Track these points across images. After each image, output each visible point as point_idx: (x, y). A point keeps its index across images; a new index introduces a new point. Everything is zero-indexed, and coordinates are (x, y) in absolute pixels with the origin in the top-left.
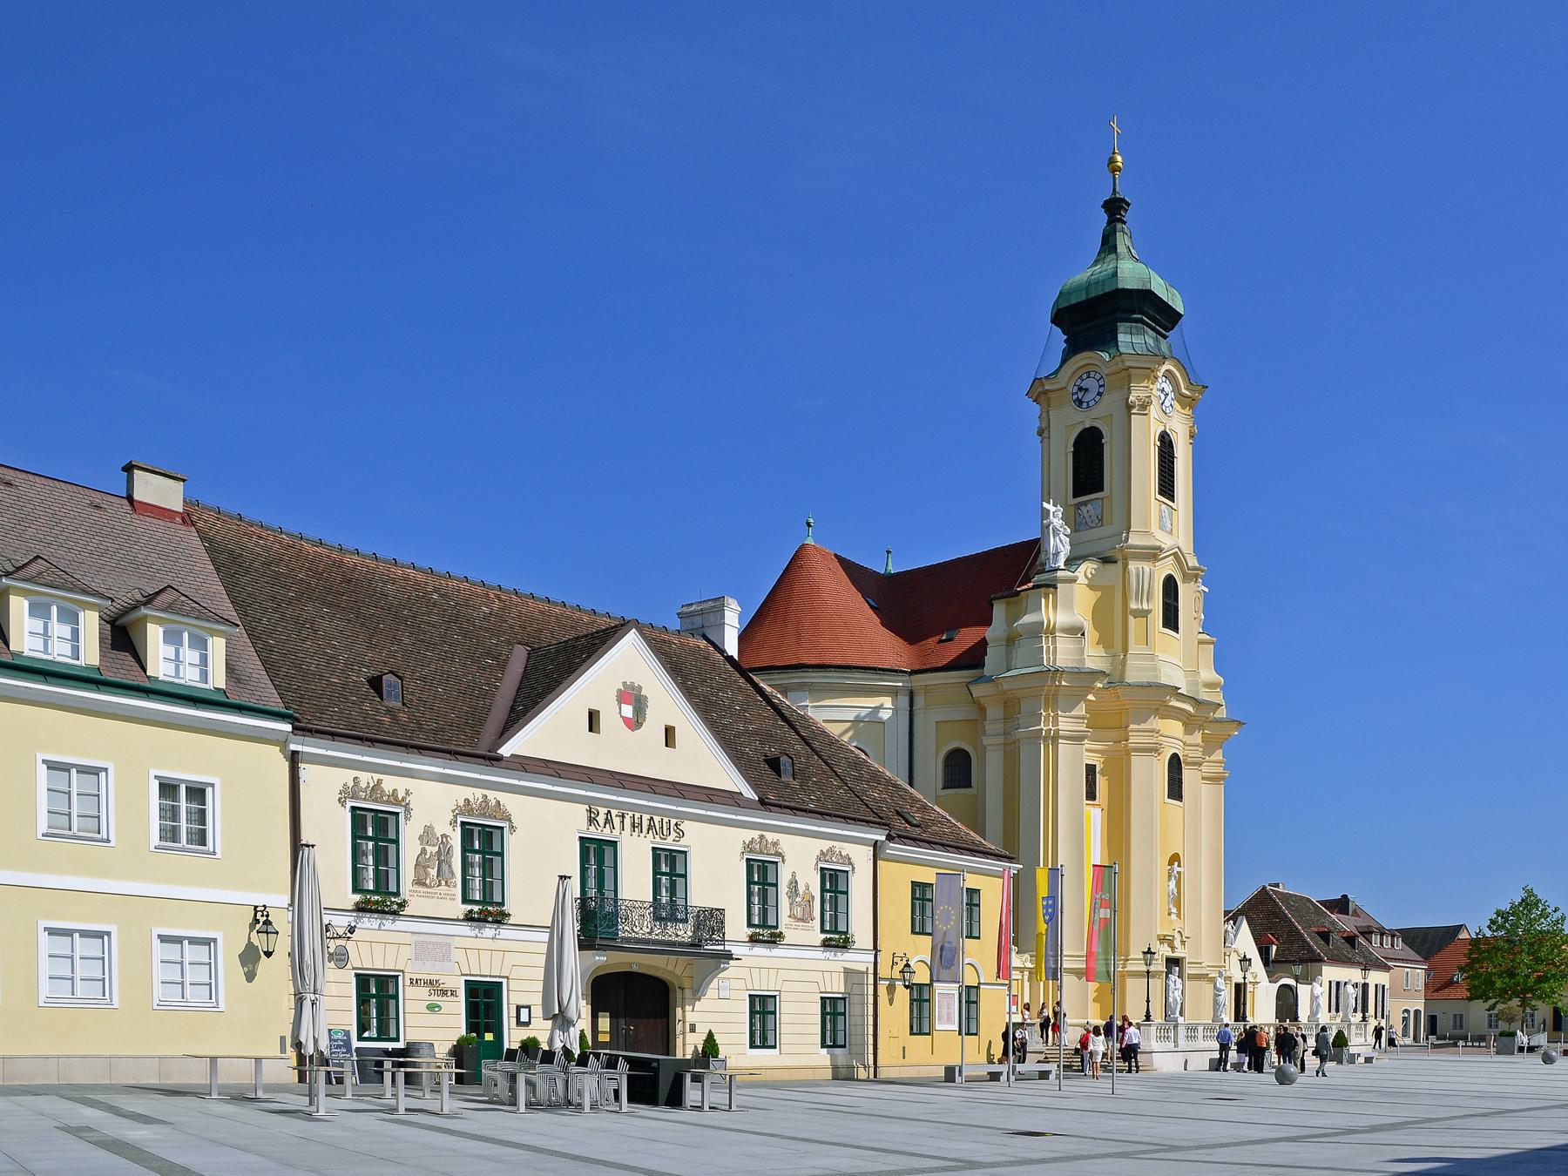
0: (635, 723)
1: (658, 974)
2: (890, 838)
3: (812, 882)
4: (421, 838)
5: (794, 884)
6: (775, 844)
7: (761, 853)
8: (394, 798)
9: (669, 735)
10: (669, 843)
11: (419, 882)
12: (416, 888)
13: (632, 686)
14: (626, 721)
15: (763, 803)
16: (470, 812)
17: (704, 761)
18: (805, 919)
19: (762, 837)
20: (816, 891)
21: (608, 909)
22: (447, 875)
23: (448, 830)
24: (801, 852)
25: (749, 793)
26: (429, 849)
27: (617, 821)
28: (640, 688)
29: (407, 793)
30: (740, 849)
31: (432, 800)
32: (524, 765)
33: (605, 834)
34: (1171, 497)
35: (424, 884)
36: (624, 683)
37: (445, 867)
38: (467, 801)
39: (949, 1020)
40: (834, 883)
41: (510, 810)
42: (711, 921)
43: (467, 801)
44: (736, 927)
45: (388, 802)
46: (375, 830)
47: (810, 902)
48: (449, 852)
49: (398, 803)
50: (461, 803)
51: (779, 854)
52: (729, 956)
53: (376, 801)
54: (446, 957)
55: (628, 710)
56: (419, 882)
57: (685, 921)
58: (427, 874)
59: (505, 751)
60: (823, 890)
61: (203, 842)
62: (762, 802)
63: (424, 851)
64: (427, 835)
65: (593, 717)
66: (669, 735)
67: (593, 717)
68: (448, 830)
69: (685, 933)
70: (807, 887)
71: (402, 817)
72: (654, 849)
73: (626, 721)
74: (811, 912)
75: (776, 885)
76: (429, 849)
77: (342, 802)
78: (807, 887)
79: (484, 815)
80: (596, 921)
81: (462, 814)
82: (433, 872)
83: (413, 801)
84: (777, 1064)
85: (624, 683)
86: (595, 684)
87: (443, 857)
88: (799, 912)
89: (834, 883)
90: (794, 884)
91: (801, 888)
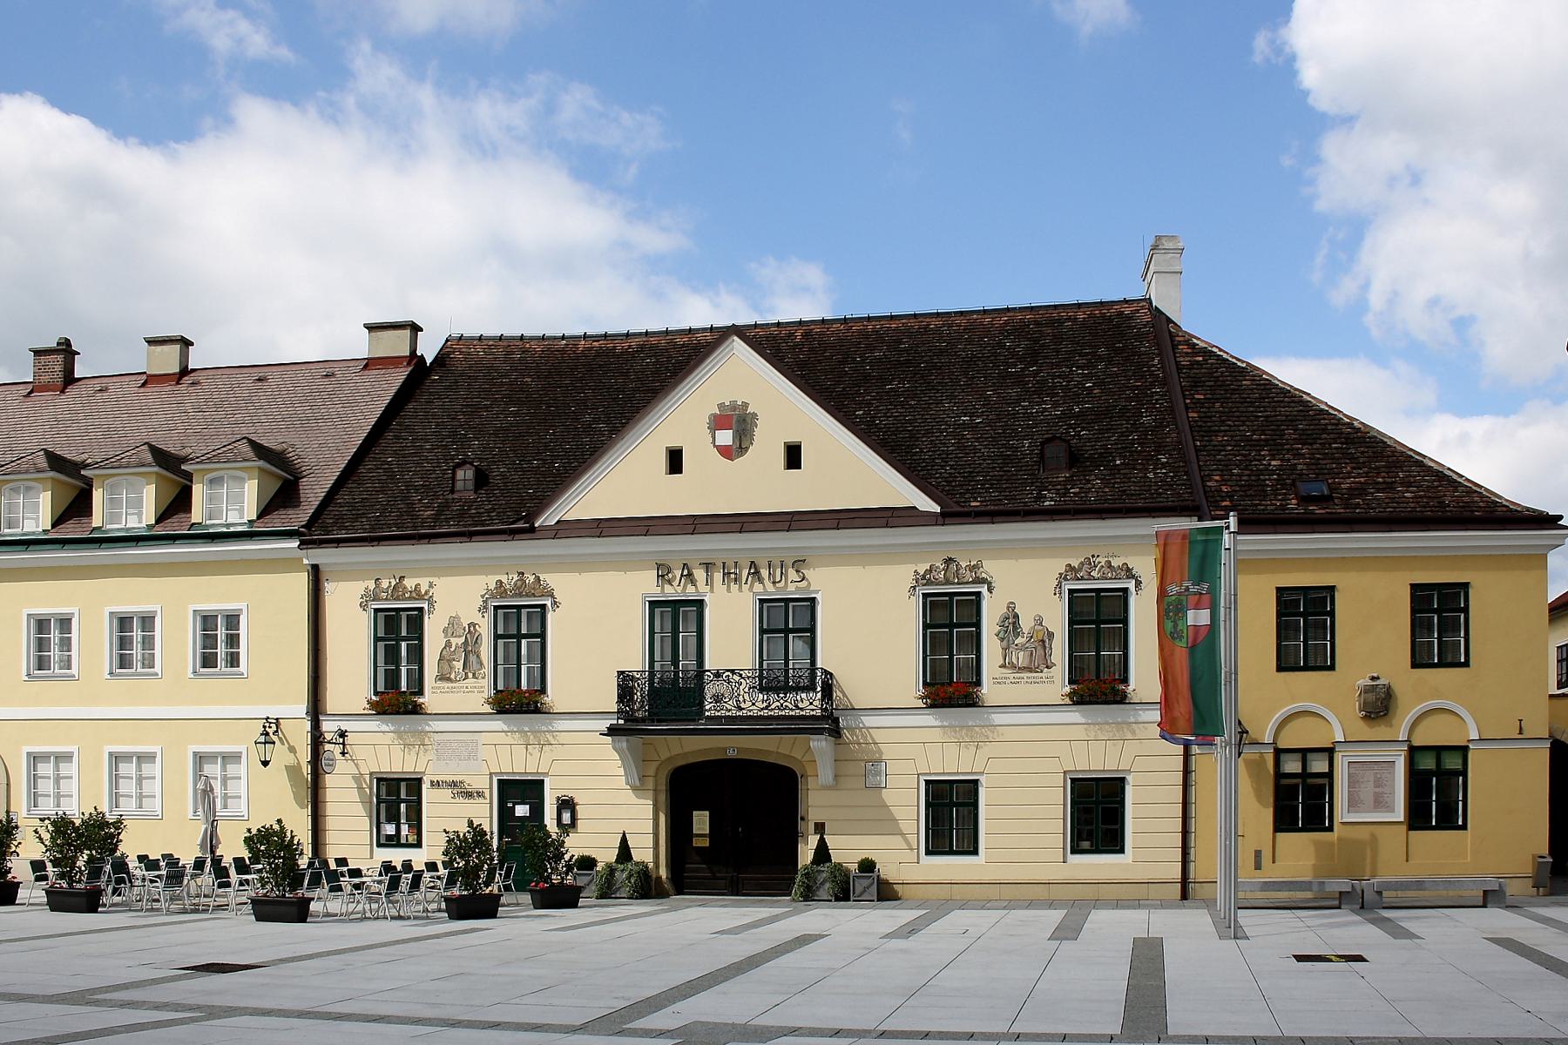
1: (771, 760)
5: (1011, 623)
6: (973, 568)
7: (947, 582)
8: (417, 594)
9: (793, 456)
10: (792, 591)
11: (442, 677)
12: (440, 684)
13: (733, 406)
15: (948, 517)
18: (1039, 662)
20: (1057, 619)
22: (475, 666)
24: (1024, 578)
26: (454, 641)
27: (700, 574)
28: (746, 405)
29: (431, 585)
30: (910, 582)
31: (456, 591)
32: (567, 529)
33: (690, 592)
35: (449, 679)
36: (721, 406)
37: (472, 658)
45: (410, 598)
46: (398, 630)
49: (420, 597)
50: (492, 586)
51: (979, 581)
53: (397, 599)
54: (472, 756)
55: (726, 437)
56: (442, 677)
59: (548, 519)
62: (943, 514)
63: (448, 644)
64: (452, 627)
65: (675, 461)
66: (793, 456)
67: (675, 461)
70: (1039, 621)
73: (726, 452)
76: (454, 641)
77: (363, 606)
78: (1039, 621)
79: (520, 595)
80: (659, 702)
81: (493, 597)
82: (459, 665)
83: (437, 593)
84: (986, 878)
85: (721, 406)
87: (470, 648)
88: (1021, 658)
90: (1011, 623)
91: (1026, 624)
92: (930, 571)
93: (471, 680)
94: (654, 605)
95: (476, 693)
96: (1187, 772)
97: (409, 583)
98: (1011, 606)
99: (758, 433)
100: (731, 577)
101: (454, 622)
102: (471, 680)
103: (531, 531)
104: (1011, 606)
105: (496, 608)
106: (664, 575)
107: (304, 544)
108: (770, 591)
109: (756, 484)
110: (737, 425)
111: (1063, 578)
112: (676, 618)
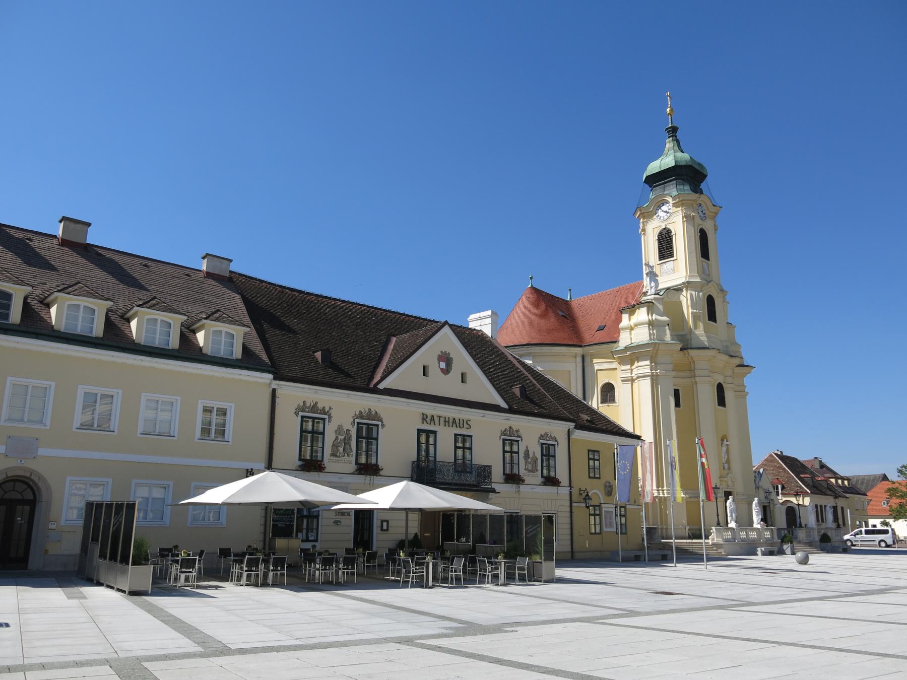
0: (446, 371)
2: (576, 427)
3: (536, 451)
4: (336, 432)
5: (527, 453)
6: (517, 431)
12: (332, 458)
13: (445, 353)
14: (442, 370)
15: (511, 411)
16: (362, 418)
17: (482, 388)
18: (533, 470)
19: (510, 428)
21: (431, 466)
23: (350, 427)
25: (504, 405)
29: (330, 408)
34: (708, 259)
35: (336, 456)
37: (347, 446)
38: (361, 412)
39: (611, 526)
40: (548, 452)
41: (382, 415)
42: (485, 472)
43: (361, 412)
44: (497, 474)
47: (535, 461)
48: (350, 438)
49: (325, 413)
52: (493, 491)
55: (443, 365)
56: (334, 454)
57: (470, 473)
58: (338, 450)
60: (542, 455)
61: (223, 434)
63: (337, 438)
64: (339, 430)
68: (350, 427)
69: (471, 479)
70: (534, 453)
71: (327, 421)
72: (456, 435)
73: (442, 370)
74: (536, 467)
75: (518, 453)
78: (534, 453)
82: (341, 449)
83: (333, 412)
86: (427, 353)
88: (530, 467)
89: (548, 452)
90: (527, 453)
91: (531, 455)
92: (506, 430)
93: (346, 457)
94: (420, 431)
95: (348, 464)
96: (571, 512)
97: (320, 406)
98: (527, 447)
99: (453, 365)
100: (447, 422)
101: (340, 428)
102: (346, 457)
103: (375, 391)
104: (527, 447)
105: (358, 423)
106: (424, 418)
107: (275, 379)
108: (459, 431)
109: (449, 386)
110: (446, 359)
111: (540, 439)
112: (426, 435)
